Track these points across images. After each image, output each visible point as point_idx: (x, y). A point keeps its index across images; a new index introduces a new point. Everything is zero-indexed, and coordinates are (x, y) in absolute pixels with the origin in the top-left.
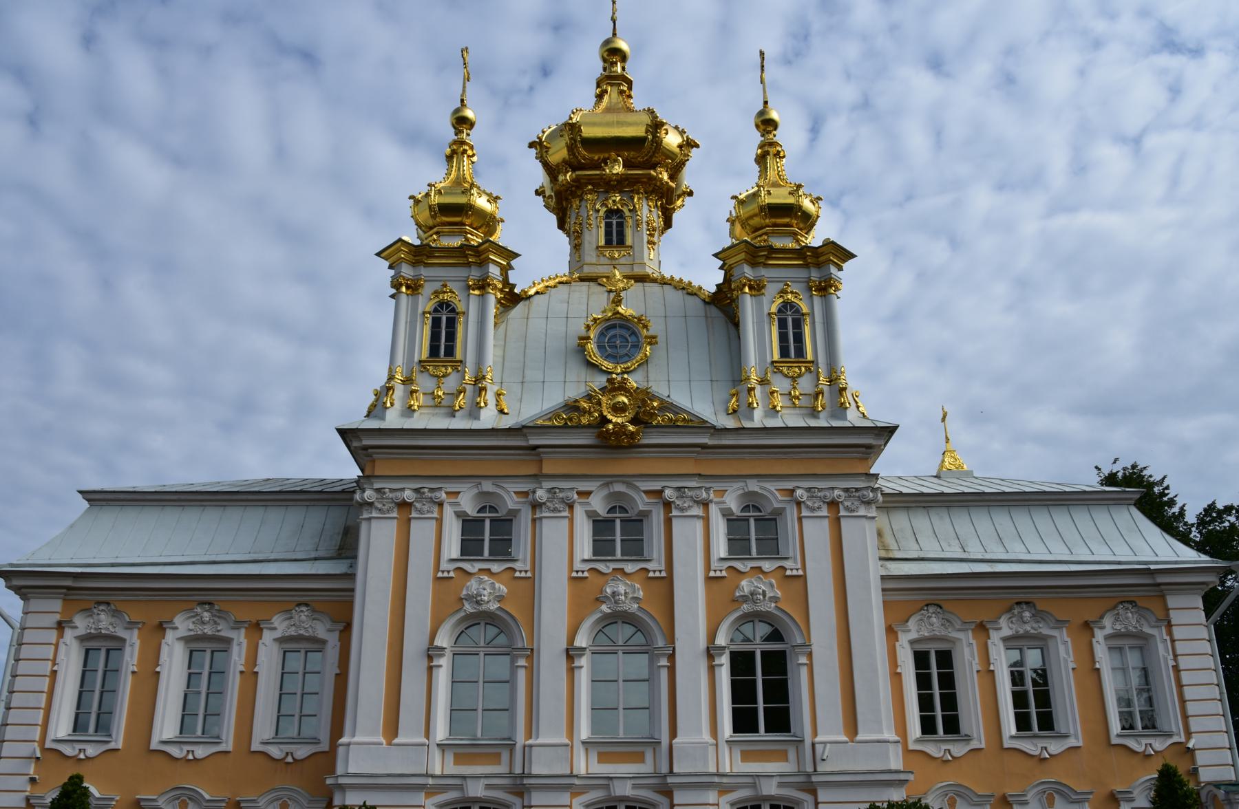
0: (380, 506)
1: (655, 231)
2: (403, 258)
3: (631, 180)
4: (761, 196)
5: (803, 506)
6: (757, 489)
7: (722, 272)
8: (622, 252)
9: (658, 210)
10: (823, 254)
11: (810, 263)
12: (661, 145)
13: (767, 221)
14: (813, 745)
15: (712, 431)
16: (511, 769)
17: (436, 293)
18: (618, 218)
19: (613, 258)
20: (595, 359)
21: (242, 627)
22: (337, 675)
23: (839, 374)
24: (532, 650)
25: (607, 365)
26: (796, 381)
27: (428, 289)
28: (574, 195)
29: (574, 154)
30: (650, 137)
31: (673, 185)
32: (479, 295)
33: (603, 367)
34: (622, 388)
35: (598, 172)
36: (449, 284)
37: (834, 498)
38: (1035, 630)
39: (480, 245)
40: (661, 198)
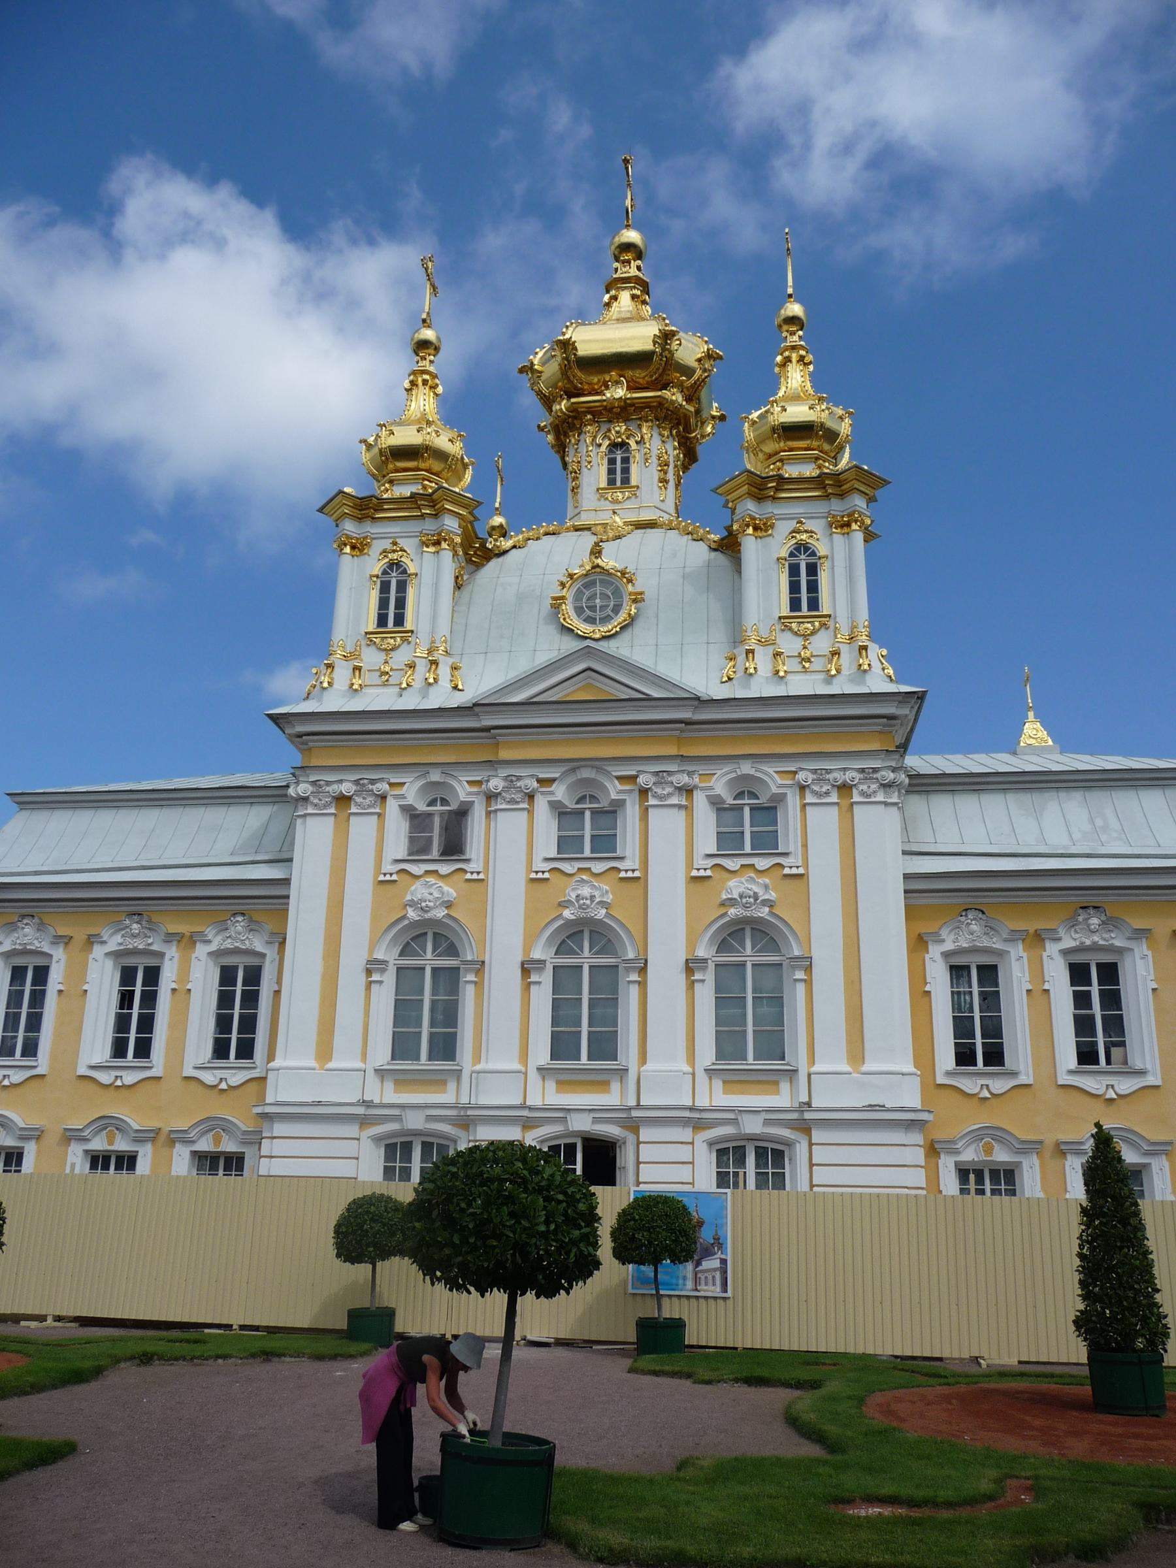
0: (316, 801)
1: (668, 466)
2: (346, 513)
5: (807, 791)
6: (752, 772)
8: (627, 493)
9: (674, 440)
10: (846, 481)
11: (831, 494)
12: (672, 360)
13: (782, 444)
14: (809, 1075)
15: (696, 703)
16: (457, 1099)
20: (570, 622)
21: (175, 940)
22: (275, 991)
24: (483, 962)
25: (583, 628)
26: (808, 640)
28: (572, 427)
29: (568, 378)
32: (434, 553)
33: (579, 632)
36: (398, 540)
37: (845, 781)
38: (1107, 941)
39: (434, 493)
40: (678, 424)
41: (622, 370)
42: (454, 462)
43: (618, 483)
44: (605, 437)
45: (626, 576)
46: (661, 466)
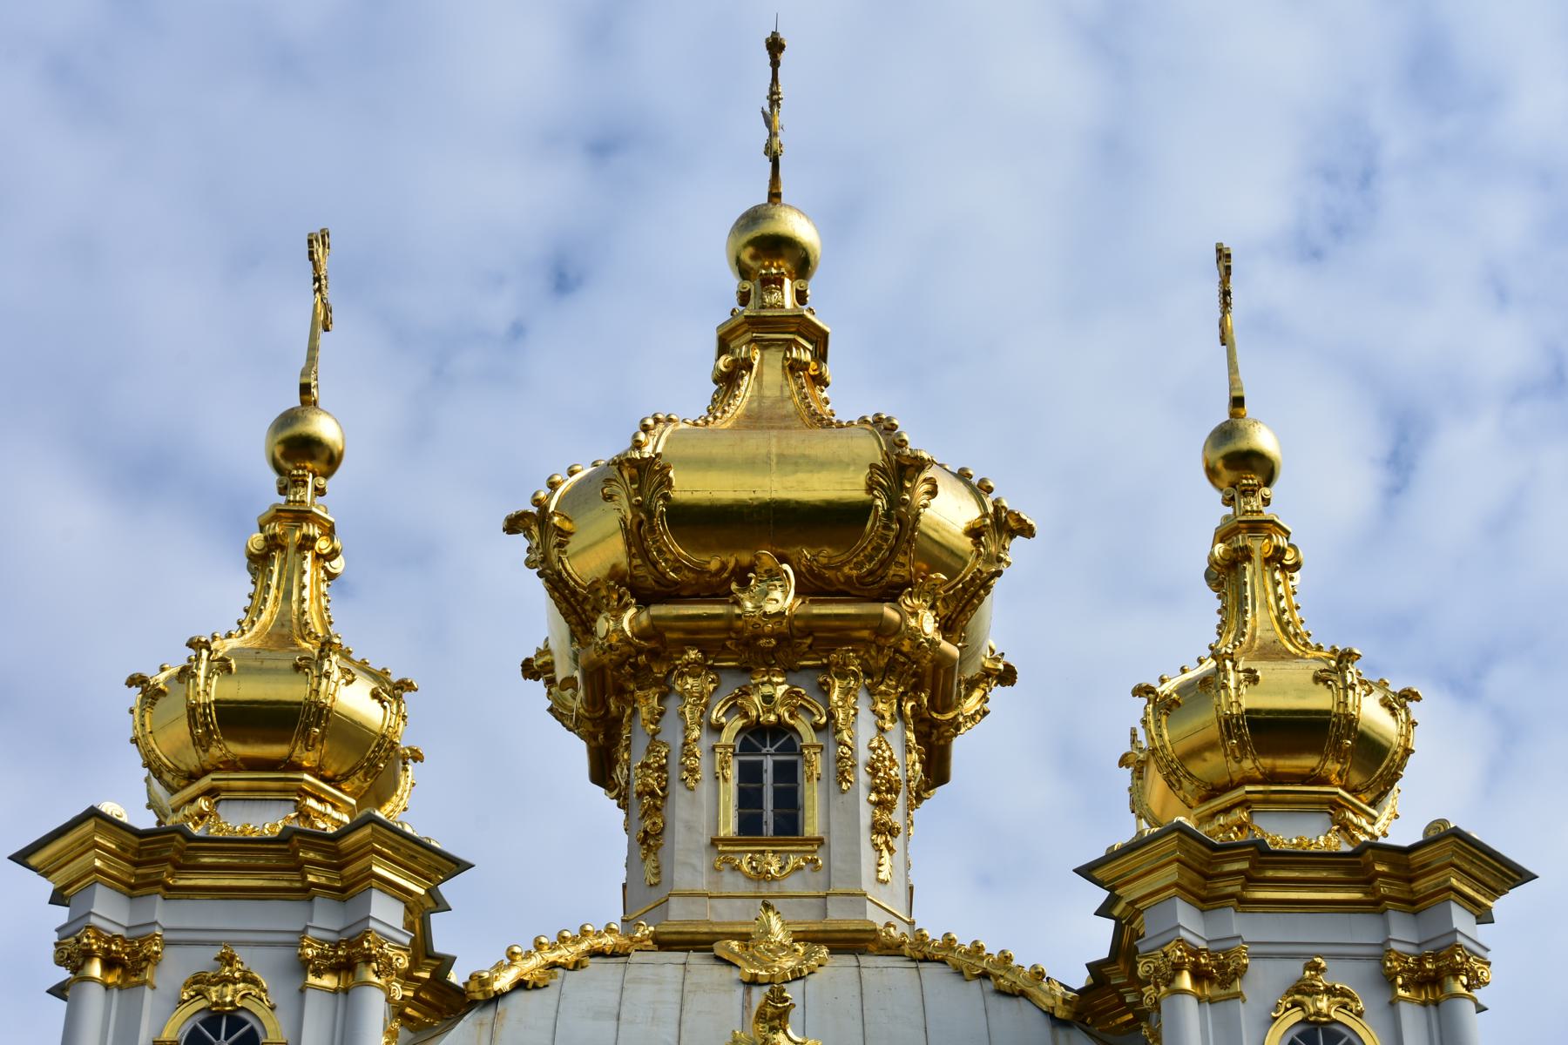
1: (897, 793)
2: (97, 870)
3: (817, 634)
4: (1225, 687)
7: (1110, 924)
8: (792, 859)
12: (914, 529)
13: (1248, 764)
17: (199, 983)
18: (780, 751)
19: (761, 876)
27: (173, 970)
28: (642, 676)
29: (644, 553)
31: (951, 649)
32: (335, 991)
35: (718, 609)
36: (240, 953)
39: (345, 831)
40: (916, 688)
41: (782, 545)
43: (769, 829)
44: (734, 709)
46: (879, 793)
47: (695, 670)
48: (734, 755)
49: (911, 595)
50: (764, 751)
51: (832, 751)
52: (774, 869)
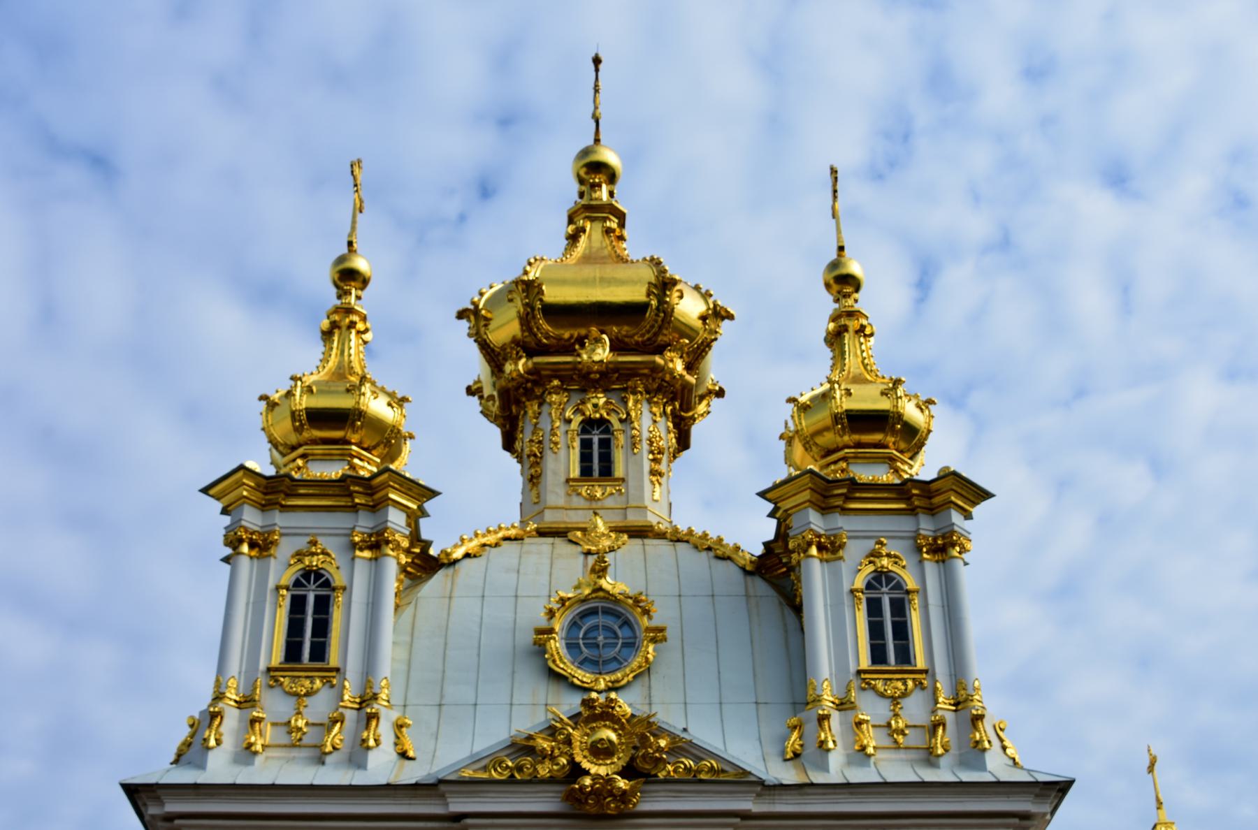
1: (663, 454)
2: (245, 497)
3: (621, 372)
4: (834, 398)
7: (774, 522)
9: (668, 419)
10: (938, 492)
11: (918, 507)
12: (671, 316)
13: (846, 438)
15: (759, 789)
17: (299, 555)
18: (601, 433)
19: (592, 498)
20: (562, 666)
23: (970, 691)
25: (582, 676)
26: (898, 703)
27: (285, 549)
28: (529, 394)
29: (530, 330)
30: (654, 303)
31: (691, 379)
32: (370, 559)
33: (576, 681)
34: (607, 715)
35: (569, 359)
36: (320, 540)
39: (374, 476)
40: (672, 401)
42: (393, 435)
43: (596, 473)
45: (641, 604)
46: (653, 454)
47: (557, 390)
48: (578, 435)
49: (670, 351)
50: (594, 433)
51: (629, 433)
52: (598, 495)
